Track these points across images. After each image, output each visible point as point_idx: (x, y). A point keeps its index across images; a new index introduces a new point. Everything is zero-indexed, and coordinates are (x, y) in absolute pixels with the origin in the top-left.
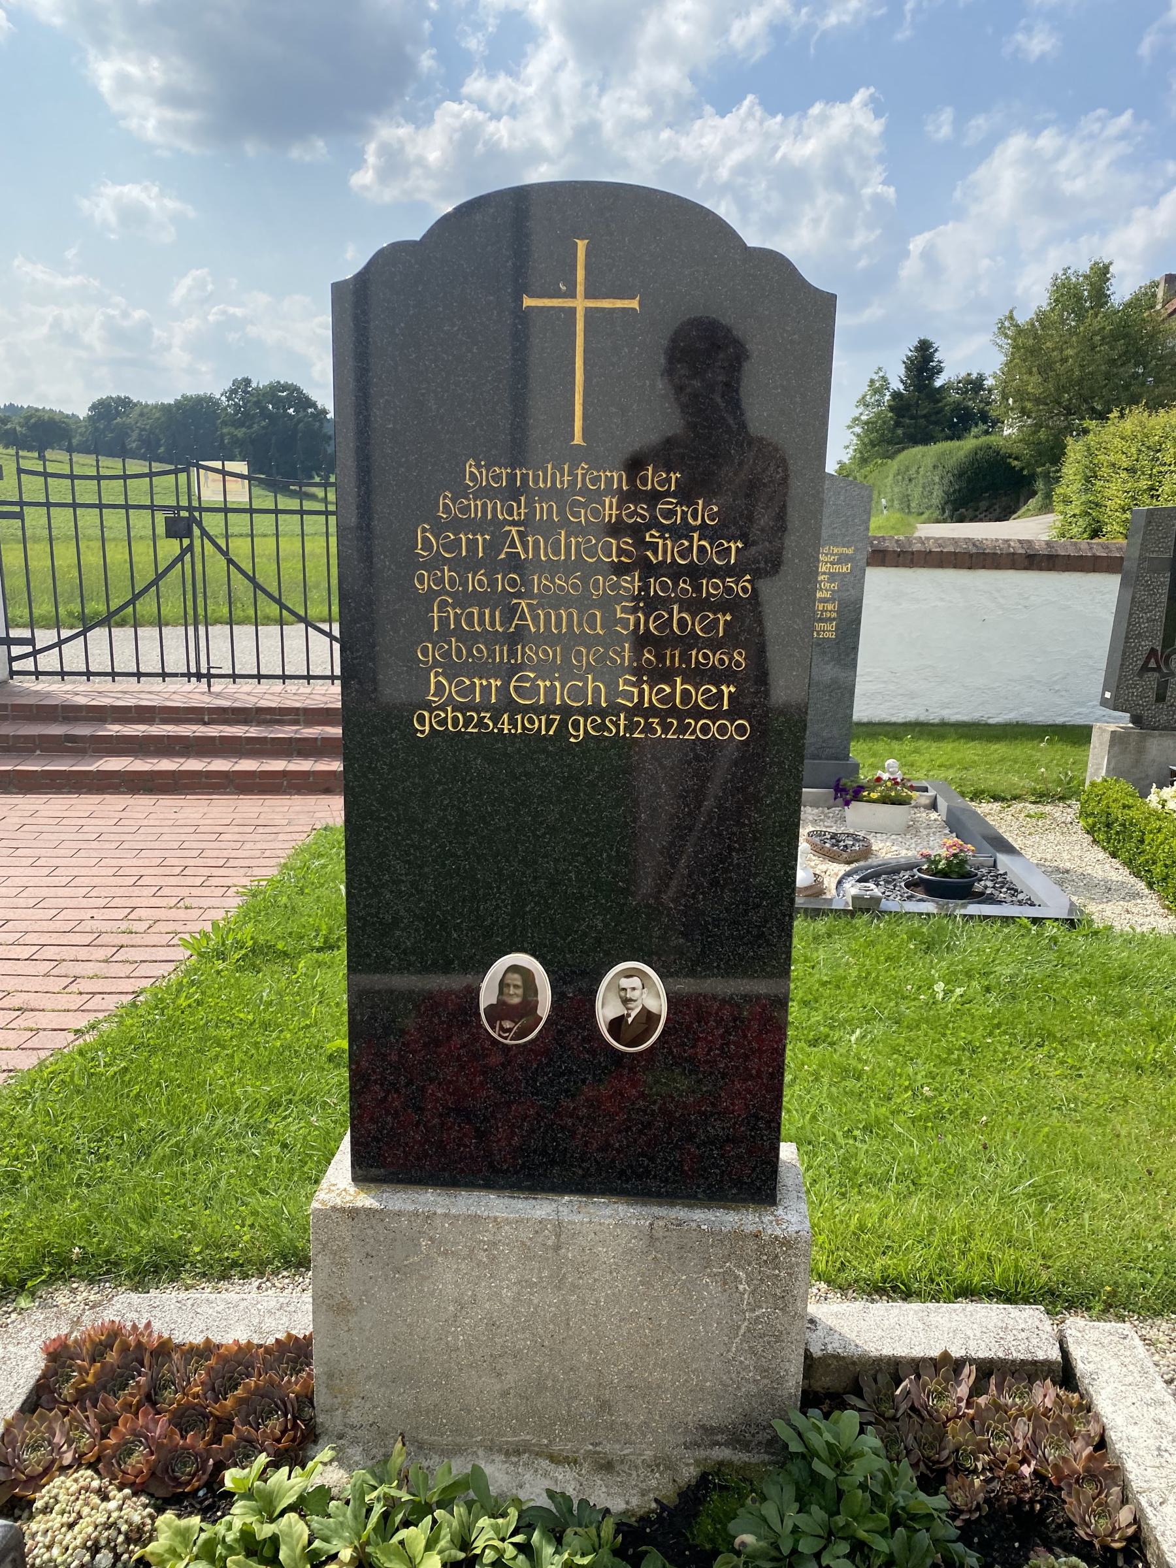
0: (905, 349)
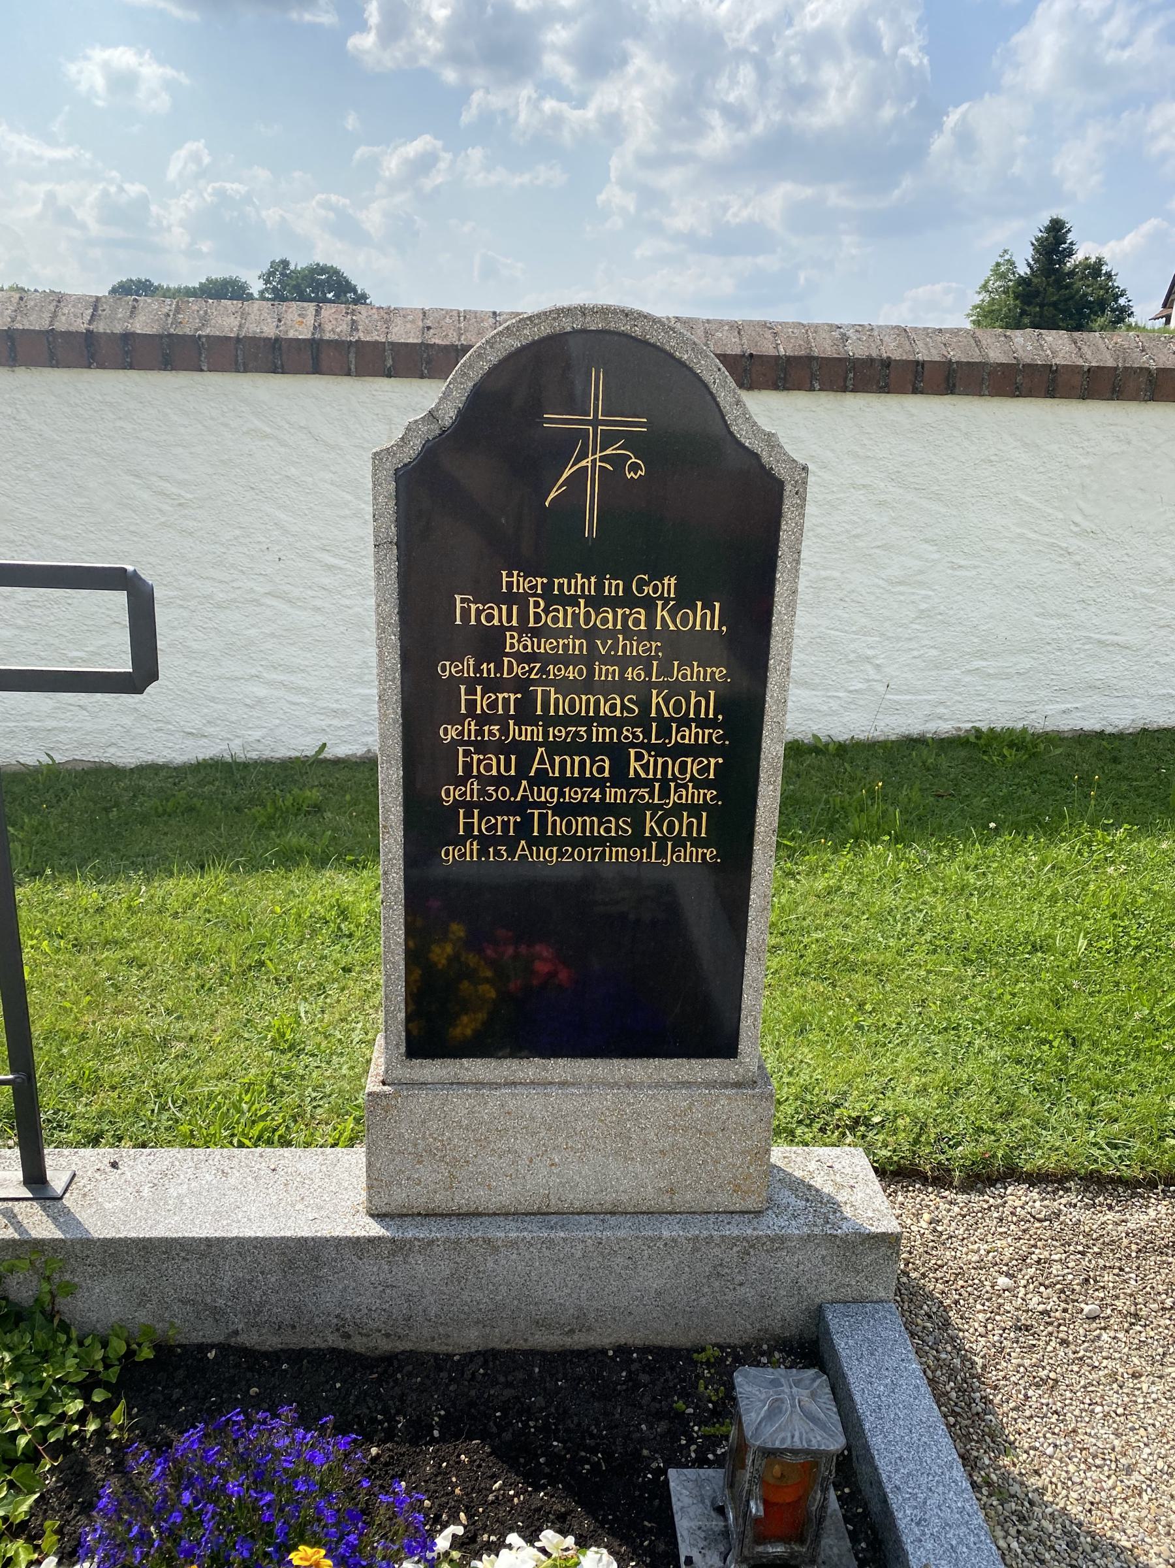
0: (1035, 226)
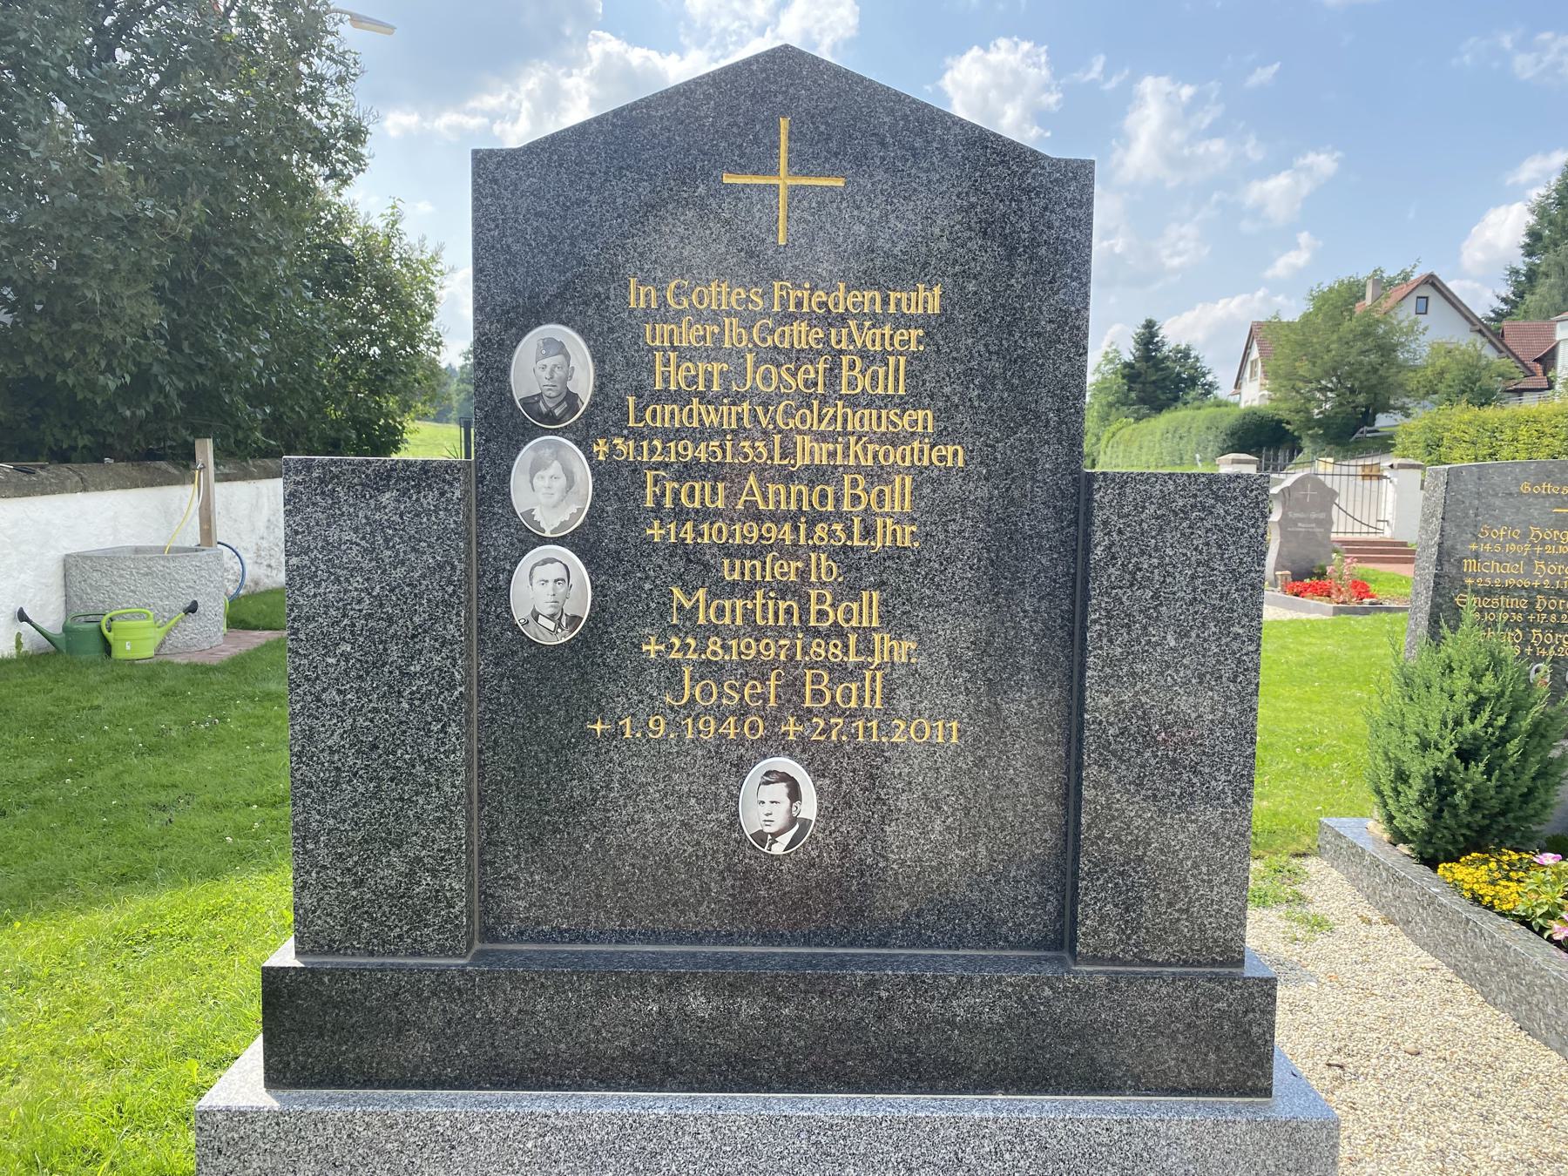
0: (1136, 328)
